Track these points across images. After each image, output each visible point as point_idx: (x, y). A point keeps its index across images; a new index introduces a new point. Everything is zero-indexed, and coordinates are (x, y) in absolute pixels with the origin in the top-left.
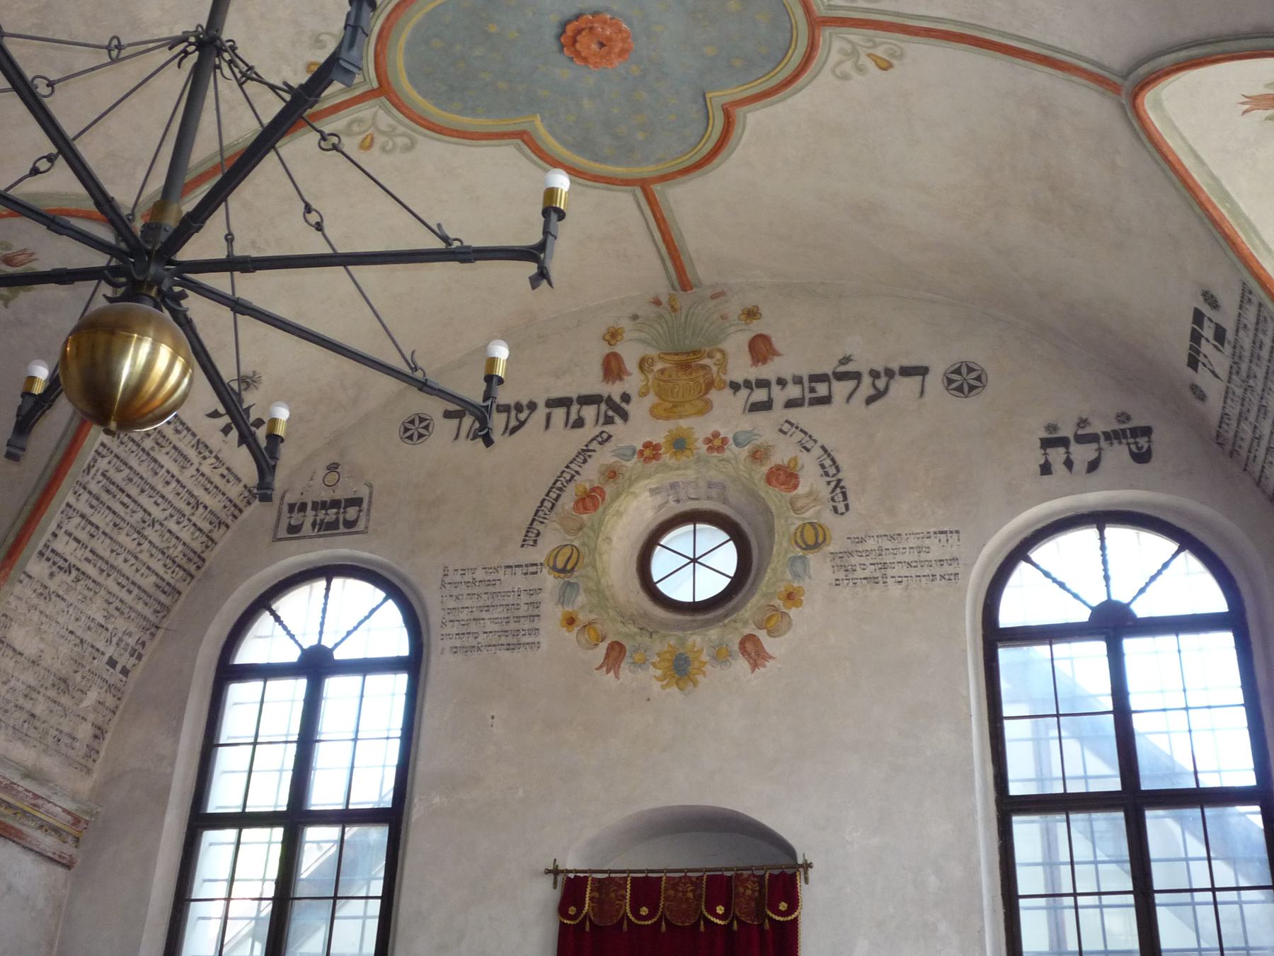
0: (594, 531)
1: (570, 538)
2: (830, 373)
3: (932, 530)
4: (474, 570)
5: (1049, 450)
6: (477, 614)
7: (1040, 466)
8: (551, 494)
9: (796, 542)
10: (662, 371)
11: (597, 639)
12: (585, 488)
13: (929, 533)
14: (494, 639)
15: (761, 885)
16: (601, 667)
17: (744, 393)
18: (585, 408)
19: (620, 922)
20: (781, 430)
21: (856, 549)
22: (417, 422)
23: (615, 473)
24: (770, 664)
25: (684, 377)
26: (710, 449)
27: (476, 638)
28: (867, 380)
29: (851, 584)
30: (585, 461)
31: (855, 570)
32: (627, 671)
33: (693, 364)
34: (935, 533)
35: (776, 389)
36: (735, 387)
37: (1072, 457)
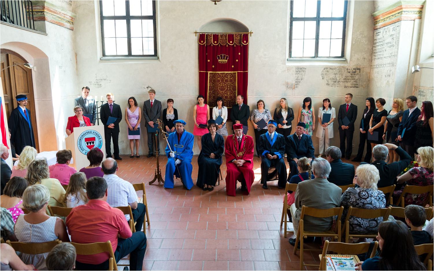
15: (241, 36)
19: (211, 44)
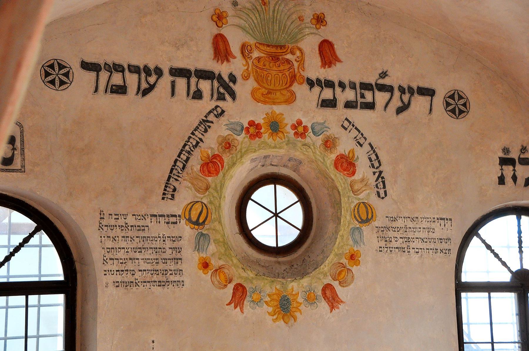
0: (217, 192)
1: (199, 195)
2: (374, 84)
3: (436, 217)
4: (125, 216)
5: (504, 167)
6: (132, 255)
7: (499, 177)
8: (182, 156)
9: (355, 217)
10: (259, 59)
11: (226, 281)
12: (208, 155)
13: (434, 218)
14: (148, 276)
16: (229, 304)
17: (317, 89)
18: (201, 81)
20: (342, 126)
21: (391, 225)
22: (56, 67)
23: (229, 144)
24: (341, 306)
25: (275, 68)
26: (296, 134)
27: (133, 274)
28: (397, 93)
29: (389, 251)
30: (206, 131)
31: (391, 241)
32: (249, 307)
33: (280, 57)
34: (438, 219)
35: (338, 90)
36: (311, 83)
37: (516, 173)
